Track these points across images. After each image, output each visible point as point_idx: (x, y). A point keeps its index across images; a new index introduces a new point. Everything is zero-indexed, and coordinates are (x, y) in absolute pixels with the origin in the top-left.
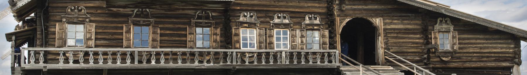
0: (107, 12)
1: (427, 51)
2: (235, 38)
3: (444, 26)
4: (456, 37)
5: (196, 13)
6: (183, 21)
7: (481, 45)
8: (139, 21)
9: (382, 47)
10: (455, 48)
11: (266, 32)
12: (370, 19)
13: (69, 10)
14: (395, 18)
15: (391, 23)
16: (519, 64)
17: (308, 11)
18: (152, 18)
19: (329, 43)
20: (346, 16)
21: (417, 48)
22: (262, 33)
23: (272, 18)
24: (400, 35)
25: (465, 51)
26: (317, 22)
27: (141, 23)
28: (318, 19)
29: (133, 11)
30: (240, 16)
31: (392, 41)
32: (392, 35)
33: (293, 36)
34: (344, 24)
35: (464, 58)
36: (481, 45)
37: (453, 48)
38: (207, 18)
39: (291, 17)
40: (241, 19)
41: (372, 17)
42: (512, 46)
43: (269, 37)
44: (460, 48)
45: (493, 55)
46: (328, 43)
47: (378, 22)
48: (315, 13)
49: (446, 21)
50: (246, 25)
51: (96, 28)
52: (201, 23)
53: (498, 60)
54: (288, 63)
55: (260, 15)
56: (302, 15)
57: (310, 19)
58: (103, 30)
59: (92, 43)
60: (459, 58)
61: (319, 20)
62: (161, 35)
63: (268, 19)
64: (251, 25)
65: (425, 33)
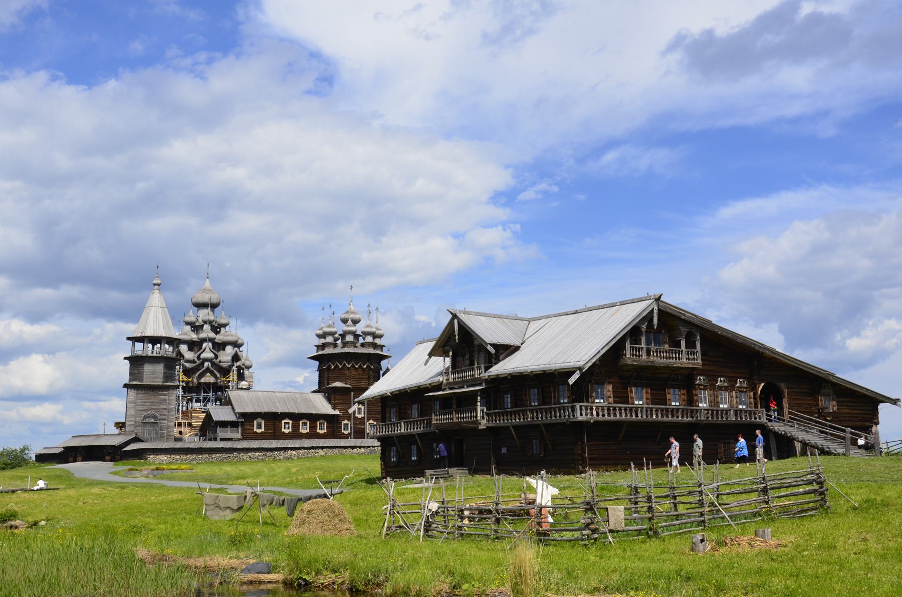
2: (695, 398)
3: (827, 390)
10: (835, 409)
26: (745, 385)
33: (731, 397)
34: (761, 387)
37: (833, 409)
44: (838, 409)
45: (858, 416)
46: (753, 403)
54: (734, 419)
59: (611, 400)
63: (714, 382)
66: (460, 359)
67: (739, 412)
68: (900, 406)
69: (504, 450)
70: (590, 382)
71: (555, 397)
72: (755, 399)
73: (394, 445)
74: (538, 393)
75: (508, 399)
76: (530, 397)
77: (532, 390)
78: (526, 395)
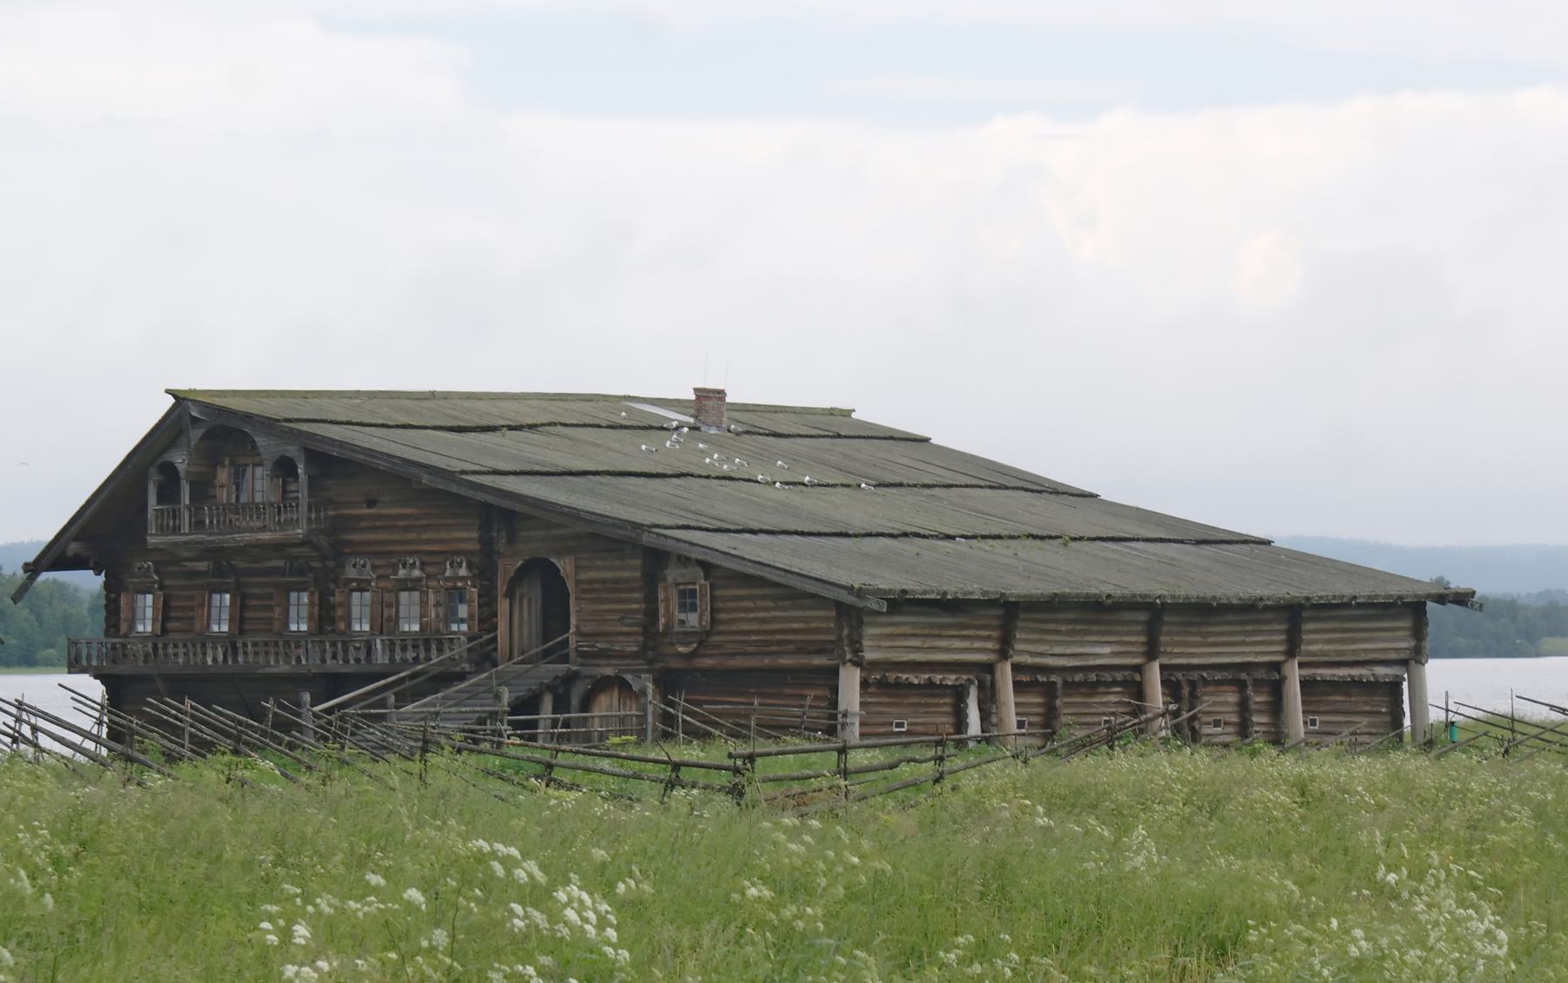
13: (136, 570)
24: (604, 595)
25: (734, 628)
38: (301, 573)
48: (458, 553)
55: (377, 562)
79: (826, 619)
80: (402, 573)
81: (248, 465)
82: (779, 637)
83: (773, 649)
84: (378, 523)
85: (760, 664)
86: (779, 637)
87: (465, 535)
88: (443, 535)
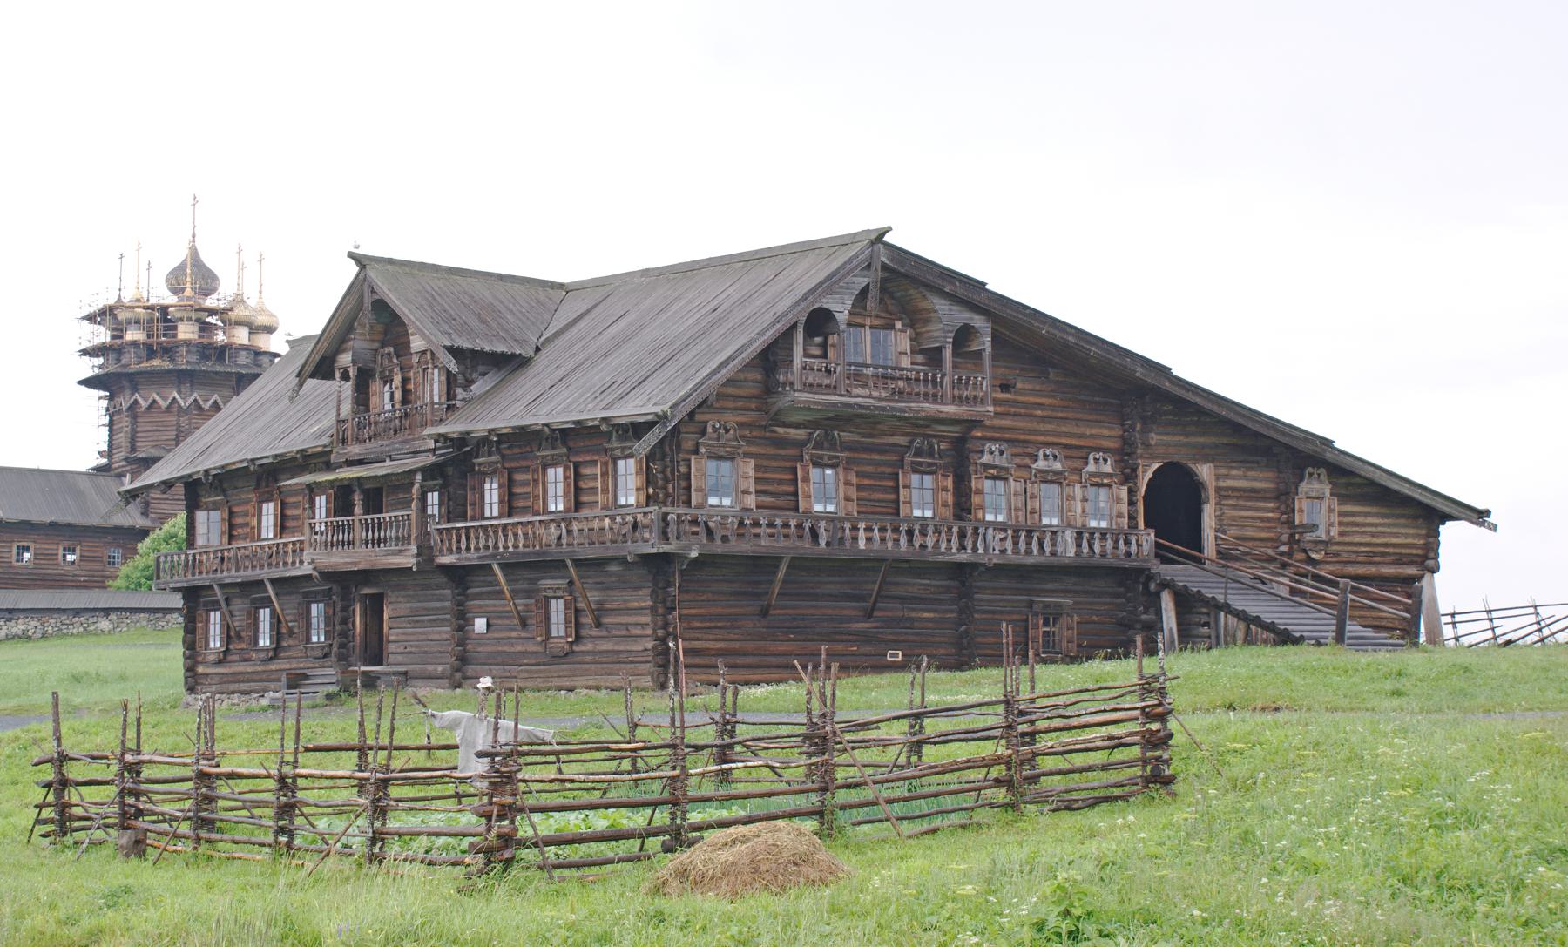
0: (768, 434)
1: (1289, 538)
2: (975, 499)
3: (1316, 485)
4: (1334, 510)
5: (911, 442)
6: (888, 458)
7: (1373, 529)
8: (821, 457)
9: (1211, 527)
10: (1332, 534)
11: (1025, 489)
12: (1193, 466)
14: (1234, 465)
15: (1226, 476)
16: (1434, 570)
17: (1091, 445)
18: (842, 451)
19: (1129, 514)
20: (1153, 458)
21: (1269, 529)
22: (1019, 490)
23: (1035, 458)
26: (1108, 469)
27: (826, 461)
28: (1109, 462)
29: (811, 434)
30: (982, 452)
31: (1229, 512)
32: (1231, 502)
34: (1149, 475)
35: (1345, 555)
36: (1373, 529)
37: (1328, 532)
39: (1066, 457)
40: (986, 459)
41: (1196, 461)
42: (1424, 532)
43: (1031, 498)
44: (1341, 534)
46: (1126, 515)
47: (1205, 472)
49: (1319, 475)
50: (992, 471)
51: (757, 468)
52: (920, 464)
53: (1399, 561)
56: (1082, 453)
57: (1096, 460)
58: (764, 472)
59: (751, 501)
60: (1336, 554)
61: (1112, 465)
62: (860, 488)
63: (1027, 461)
64: (1000, 475)
65: (1284, 496)
66: (376, 386)
67: (1086, 536)
68: (1494, 528)
69: (480, 624)
70: (696, 452)
71: (605, 490)
72: (1131, 503)
73: (215, 606)
74: (566, 478)
75: (492, 493)
76: (545, 491)
77: (551, 471)
78: (536, 482)
79: (1418, 536)
80: (1041, 464)
81: (863, 326)
82: (1382, 549)
83: (1376, 559)
84: (1013, 410)
85: (1368, 572)
86: (1382, 549)
87: (1106, 432)
88: (1082, 430)
